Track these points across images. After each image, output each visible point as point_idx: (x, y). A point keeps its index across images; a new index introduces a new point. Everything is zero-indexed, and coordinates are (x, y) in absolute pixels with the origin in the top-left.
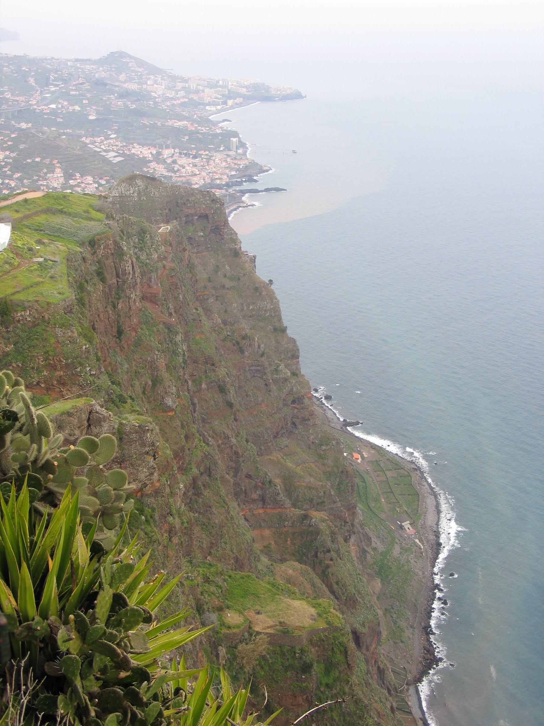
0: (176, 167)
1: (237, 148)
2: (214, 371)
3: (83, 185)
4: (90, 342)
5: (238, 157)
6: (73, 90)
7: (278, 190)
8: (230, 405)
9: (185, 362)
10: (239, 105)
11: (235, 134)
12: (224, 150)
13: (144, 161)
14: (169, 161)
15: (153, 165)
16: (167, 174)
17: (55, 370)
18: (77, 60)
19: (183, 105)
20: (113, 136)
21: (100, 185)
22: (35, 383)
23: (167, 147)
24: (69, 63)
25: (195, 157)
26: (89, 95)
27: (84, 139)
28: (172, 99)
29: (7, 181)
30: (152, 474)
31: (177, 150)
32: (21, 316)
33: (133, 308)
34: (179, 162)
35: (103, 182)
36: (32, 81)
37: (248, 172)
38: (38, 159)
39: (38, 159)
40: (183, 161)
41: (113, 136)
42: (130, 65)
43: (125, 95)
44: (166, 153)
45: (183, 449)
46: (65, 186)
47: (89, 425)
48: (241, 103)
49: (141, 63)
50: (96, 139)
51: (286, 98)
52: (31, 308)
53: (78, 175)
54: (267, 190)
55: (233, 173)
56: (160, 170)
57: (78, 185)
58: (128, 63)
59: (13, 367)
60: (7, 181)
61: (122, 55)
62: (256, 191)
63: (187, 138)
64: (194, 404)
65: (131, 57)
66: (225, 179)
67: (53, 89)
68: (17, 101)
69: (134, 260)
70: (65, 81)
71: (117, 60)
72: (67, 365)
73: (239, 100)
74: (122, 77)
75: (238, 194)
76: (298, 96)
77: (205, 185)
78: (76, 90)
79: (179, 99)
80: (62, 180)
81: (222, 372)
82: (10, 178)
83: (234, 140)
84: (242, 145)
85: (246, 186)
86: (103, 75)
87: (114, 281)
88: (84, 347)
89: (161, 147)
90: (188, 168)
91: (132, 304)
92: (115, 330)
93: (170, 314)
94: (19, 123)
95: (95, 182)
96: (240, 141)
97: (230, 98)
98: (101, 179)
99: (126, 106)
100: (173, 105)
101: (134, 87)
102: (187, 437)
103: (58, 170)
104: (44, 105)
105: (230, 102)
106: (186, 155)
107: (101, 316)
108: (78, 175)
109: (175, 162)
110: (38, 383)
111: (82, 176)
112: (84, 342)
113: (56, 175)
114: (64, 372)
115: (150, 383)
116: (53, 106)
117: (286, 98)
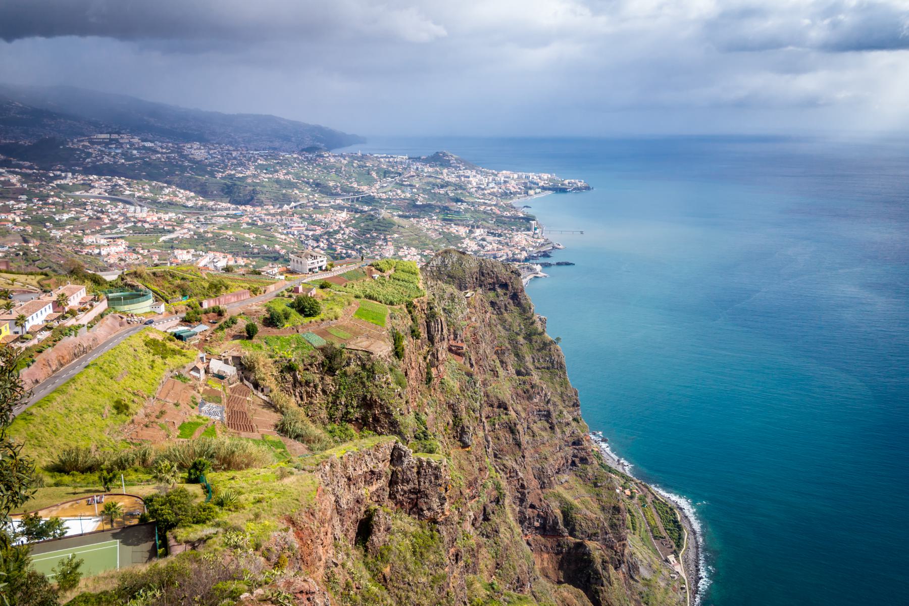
0: (484, 243)
1: (535, 229)
2: (506, 414)
7: (567, 264)
8: (518, 444)
9: (481, 406)
13: (459, 239)
15: (467, 241)
23: (478, 227)
25: (500, 235)
28: (483, 189)
30: (442, 504)
31: (486, 230)
33: (440, 358)
36: (374, 174)
37: (543, 249)
38: (375, 234)
40: (490, 238)
45: (476, 479)
53: (405, 248)
54: (558, 264)
55: (531, 249)
62: (550, 265)
64: (488, 442)
66: (524, 255)
69: (443, 319)
70: (400, 174)
73: (538, 190)
77: (508, 260)
80: (392, 252)
81: (512, 413)
83: (533, 222)
87: (426, 335)
89: (473, 227)
91: (439, 355)
92: (425, 375)
93: (472, 365)
97: (531, 188)
102: (480, 470)
103: (389, 243)
105: (531, 192)
106: (492, 233)
107: (413, 364)
108: (405, 248)
115: (451, 422)
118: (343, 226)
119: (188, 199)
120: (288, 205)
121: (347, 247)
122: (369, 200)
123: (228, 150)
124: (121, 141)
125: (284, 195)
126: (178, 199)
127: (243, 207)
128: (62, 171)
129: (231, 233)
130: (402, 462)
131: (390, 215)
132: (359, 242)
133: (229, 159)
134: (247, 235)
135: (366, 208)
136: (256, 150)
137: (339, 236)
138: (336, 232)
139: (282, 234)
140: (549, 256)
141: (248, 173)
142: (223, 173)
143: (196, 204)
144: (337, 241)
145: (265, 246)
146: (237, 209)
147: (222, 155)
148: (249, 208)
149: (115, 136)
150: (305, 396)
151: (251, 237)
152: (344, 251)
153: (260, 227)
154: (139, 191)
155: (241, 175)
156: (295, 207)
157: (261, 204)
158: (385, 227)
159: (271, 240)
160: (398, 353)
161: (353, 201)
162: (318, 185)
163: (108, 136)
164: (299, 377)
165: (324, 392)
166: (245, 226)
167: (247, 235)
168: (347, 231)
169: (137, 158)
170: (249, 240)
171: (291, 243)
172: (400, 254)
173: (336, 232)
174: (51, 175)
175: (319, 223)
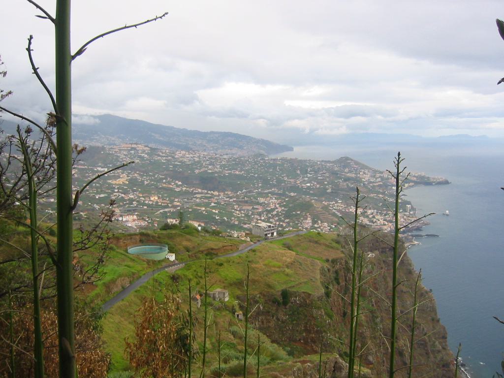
0: (375, 220)
1: (410, 211)
3: (322, 227)
4: (331, 319)
5: (411, 216)
6: (319, 176)
8: (405, 364)
10: (412, 186)
11: (409, 203)
12: (402, 212)
14: (371, 216)
16: (369, 223)
17: (310, 333)
18: (323, 161)
19: (380, 186)
20: (340, 201)
21: (331, 228)
22: (298, 340)
23: (370, 209)
24: (318, 163)
25: (385, 215)
26: (328, 179)
27: (324, 202)
28: (373, 182)
29: (281, 223)
31: (375, 211)
32: (294, 300)
34: (377, 217)
35: (334, 227)
36: (299, 172)
38: (299, 212)
39: (299, 212)
40: (378, 217)
41: (340, 201)
42: (351, 163)
43: (347, 179)
44: (369, 212)
46: (313, 227)
47: (334, 371)
48: (413, 186)
49: (357, 163)
50: (330, 203)
51: (440, 183)
52: (299, 296)
53: (319, 222)
54: (427, 235)
56: (366, 221)
57: (319, 227)
58: (350, 163)
59: (287, 329)
60: (281, 223)
61: (347, 158)
63: (381, 204)
64: (384, 361)
65: (352, 160)
67: (309, 175)
68: (290, 181)
71: (344, 162)
72: (317, 331)
73: (411, 184)
74: (347, 170)
75: (410, 237)
76: (446, 182)
78: (321, 177)
79: (377, 183)
80: (311, 224)
82: (283, 221)
83: (409, 206)
84: (413, 209)
85: (415, 233)
86: (336, 169)
87: (344, 284)
88: (327, 321)
90: (381, 221)
92: (342, 312)
93: (373, 305)
94: (290, 193)
95: (329, 226)
96: (412, 207)
98: (332, 224)
99: (347, 185)
100: (374, 186)
101: (353, 175)
103: (309, 219)
104: (305, 184)
106: (380, 213)
107: (336, 303)
108: (319, 222)
109: (374, 217)
110: (300, 340)
111: (322, 222)
112: (327, 318)
113: (307, 221)
114: (315, 335)
116: (309, 185)
117: (440, 183)
118: (277, 206)
119: (178, 186)
120: (241, 191)
121: (280, 220)
122: (294, 188)
123: (204, 155)
124: (137, 149)
125: (239, 184)
126: (171, 186)
127: (212, 192)
128: (102, 168)
129: (204, 209)
130: (341, 372)
131: (309, 200)
132: (286, 217)
133: (204, 161)
134: (214, 211)
135: (292, 194)
136: (221, 155)
137: (275, 213)
138: (273, 210)
139: (236, 210)
140: (421, 230)
141: (216, 170)
142: (199, 169)
143: (182, 190)
144: (273, 216)
145: (226, 218)
146: (207, 193)
147: (200, 158)
148: (216, 193)
149: (134, 146)
150: (265, 321)
151: (217, 212)
152: (278, 223)
153: (223, 205)
154: (147, 181)
155: (210, 171)
156: (246, 192)
157: (223, 191)
158: (306, 207)
159: (230, 215)
160: (328, 295)
161: (284, 190)
162: (261, 178)
163: (130, 146)
164: (261, 308)
165: (278, 319)
166: (213, 204)
167: (214, 211)
168: (280, 210)
169: (147, 160)
170: (215, 214)
171: (242, 217)
172: (316, 225)
173: (273, 210)
174: (95, 169)
175: (261, 204)
